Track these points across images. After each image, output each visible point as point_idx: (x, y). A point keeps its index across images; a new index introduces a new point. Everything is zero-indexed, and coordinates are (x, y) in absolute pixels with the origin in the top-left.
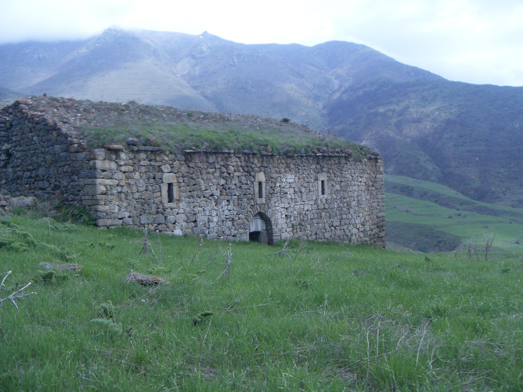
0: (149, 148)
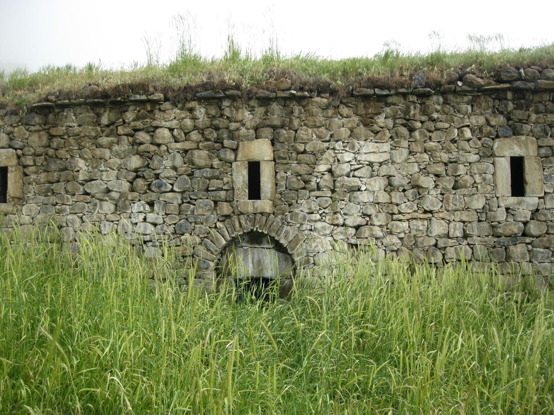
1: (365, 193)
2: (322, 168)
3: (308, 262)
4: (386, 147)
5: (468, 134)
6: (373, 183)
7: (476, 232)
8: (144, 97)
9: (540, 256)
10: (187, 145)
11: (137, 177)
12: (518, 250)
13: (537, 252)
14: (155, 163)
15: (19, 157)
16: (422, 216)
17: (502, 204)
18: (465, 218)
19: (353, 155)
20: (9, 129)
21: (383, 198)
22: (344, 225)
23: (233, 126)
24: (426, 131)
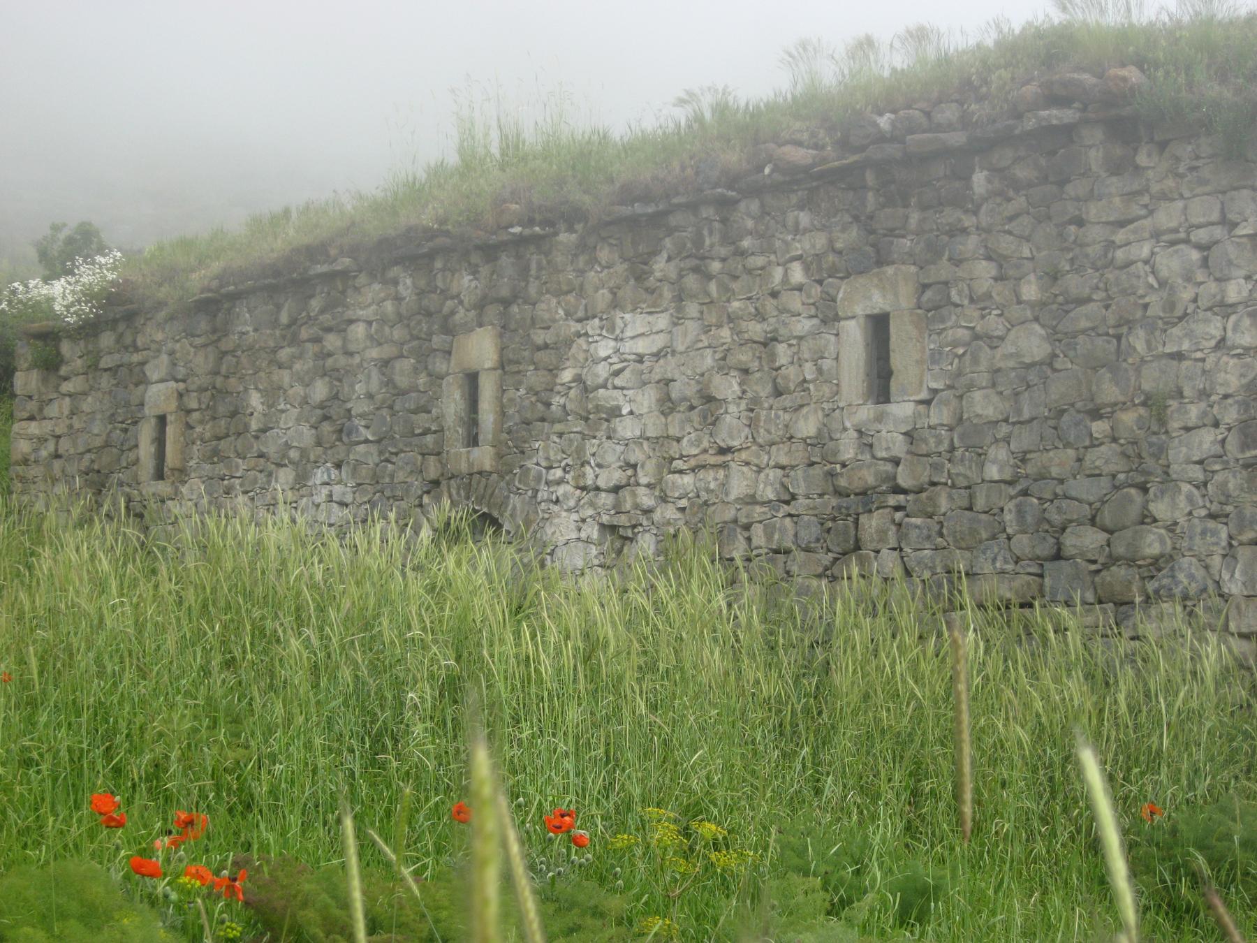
1: (628, 421)
2: (567, 376)
4: (662, 321)
5: (797, 274)
6: (639, 398)
9: (914, 534)
12: (872, 523)
15: (180, 395)
16: (713, 460)
17: (848, 425)
18: (784, 460)
19: (612, 343)
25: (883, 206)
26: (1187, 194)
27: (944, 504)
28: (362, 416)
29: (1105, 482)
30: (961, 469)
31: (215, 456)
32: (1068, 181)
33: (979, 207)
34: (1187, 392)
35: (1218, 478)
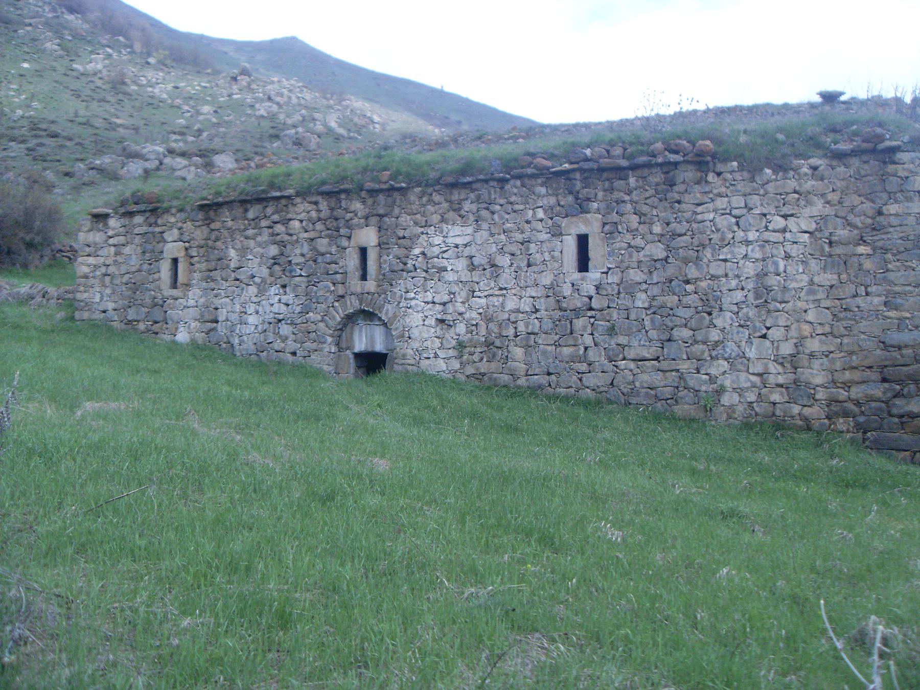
0: (142, 207)
2: (417, 251)
3: (403, 336)
4: (469, 230)
5: (540, 214)
6: (457, 263)
7: (543, 307)
8: (278, 194)
9: (600, 328)
10: (312, 235)
11: (275, 264)
12: (579, 323)
13: (598, 325)
14: (288, 251)
15: (186, 249)
16: (497, 293)
18: (534, 294)
20: (180, 225)
21: (465, 276)
22: (433, 302)
23: (349, 216)
24: (503, 213)
25: (583, 188)
26: (729, 194)
27: (615, 316)
28: (297, 264)
29: (692, 310)
30: (624, 302)
31: (207, 279)
32: (675, 185)
33: (631, 192)
34: (730, 275)
35: (745, 310)
